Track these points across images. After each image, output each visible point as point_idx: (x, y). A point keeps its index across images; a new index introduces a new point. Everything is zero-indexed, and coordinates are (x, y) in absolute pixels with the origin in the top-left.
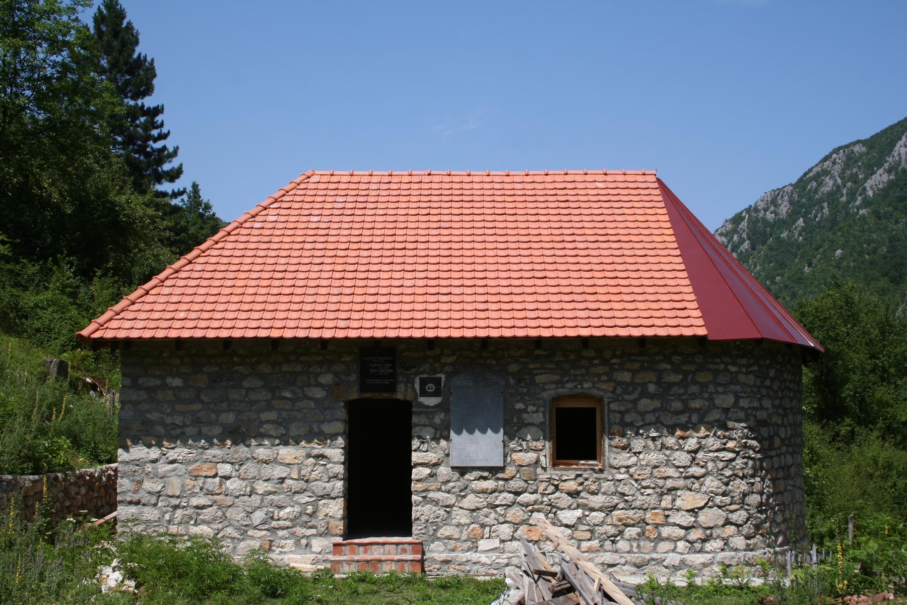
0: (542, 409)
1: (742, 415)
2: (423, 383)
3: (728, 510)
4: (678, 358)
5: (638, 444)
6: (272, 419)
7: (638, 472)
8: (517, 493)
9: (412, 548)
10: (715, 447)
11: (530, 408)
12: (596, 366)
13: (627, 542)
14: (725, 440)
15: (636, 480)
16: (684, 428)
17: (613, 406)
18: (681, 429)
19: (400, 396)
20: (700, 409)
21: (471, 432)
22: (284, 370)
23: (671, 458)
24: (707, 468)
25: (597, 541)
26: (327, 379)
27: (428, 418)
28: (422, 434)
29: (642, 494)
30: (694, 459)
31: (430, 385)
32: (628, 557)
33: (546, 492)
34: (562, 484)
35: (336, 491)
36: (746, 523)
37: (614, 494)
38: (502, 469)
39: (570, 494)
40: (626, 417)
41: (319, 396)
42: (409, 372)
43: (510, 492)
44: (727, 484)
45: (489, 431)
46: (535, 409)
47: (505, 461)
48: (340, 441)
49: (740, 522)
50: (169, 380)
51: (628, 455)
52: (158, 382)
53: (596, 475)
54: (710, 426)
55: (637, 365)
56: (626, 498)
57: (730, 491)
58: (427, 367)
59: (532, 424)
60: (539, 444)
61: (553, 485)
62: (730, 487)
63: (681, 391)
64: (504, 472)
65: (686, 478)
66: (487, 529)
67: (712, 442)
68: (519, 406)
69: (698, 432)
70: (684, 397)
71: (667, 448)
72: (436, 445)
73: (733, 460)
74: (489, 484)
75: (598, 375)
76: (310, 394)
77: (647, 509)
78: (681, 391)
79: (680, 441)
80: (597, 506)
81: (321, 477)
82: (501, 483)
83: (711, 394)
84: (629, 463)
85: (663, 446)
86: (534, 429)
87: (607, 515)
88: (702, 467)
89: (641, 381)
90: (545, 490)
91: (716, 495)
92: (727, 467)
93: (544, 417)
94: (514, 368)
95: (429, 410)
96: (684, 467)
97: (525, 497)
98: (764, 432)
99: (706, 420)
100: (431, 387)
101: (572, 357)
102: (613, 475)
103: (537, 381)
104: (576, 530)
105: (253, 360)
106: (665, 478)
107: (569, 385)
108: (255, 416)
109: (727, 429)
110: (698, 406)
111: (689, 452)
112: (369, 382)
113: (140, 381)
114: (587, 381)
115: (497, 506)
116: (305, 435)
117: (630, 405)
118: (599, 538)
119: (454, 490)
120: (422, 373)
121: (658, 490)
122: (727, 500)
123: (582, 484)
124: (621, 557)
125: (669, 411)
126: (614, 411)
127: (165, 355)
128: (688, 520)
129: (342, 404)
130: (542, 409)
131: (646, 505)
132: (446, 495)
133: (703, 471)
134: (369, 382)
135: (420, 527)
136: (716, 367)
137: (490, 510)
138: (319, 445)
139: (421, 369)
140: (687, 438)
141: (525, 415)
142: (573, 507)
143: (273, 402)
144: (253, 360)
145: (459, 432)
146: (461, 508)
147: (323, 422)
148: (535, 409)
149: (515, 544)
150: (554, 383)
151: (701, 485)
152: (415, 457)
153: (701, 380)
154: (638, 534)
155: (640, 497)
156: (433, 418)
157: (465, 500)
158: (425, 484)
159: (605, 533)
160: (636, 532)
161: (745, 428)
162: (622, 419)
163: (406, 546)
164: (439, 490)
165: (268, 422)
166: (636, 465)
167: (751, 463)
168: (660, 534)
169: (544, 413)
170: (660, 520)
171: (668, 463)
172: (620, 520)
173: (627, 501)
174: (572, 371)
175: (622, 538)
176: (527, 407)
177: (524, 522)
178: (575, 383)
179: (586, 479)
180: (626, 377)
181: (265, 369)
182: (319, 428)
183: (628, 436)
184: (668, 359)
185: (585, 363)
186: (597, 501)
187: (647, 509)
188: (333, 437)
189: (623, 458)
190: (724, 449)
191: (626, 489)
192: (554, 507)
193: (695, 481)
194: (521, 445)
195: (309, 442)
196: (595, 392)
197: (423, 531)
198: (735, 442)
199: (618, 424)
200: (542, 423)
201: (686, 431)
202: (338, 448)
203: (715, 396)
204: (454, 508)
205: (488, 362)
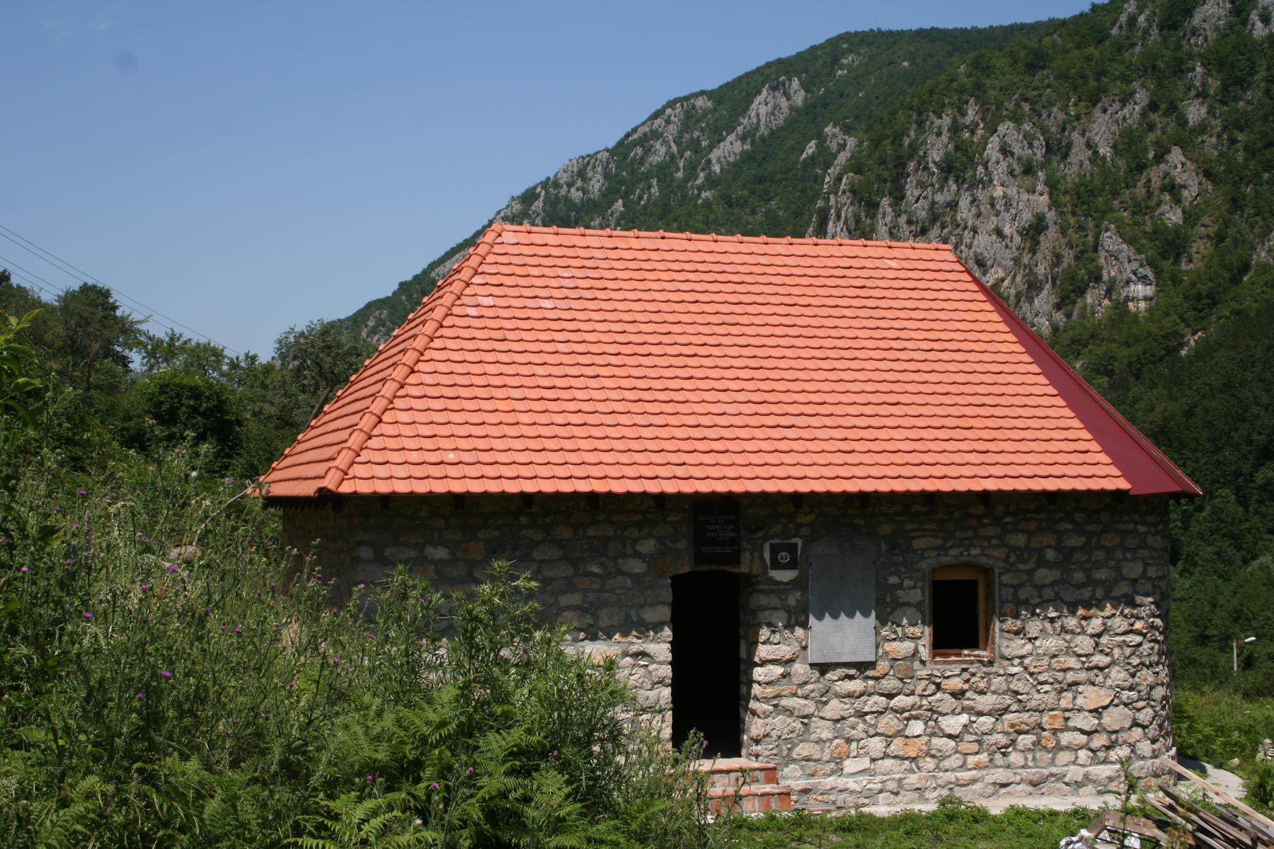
0: (920, 584)
2: (775, 550)
3: (1134, 708)
4: (1082, 515)
5: (1034, 627)
6: (575, 603)
7: (1034, 664)
8: (890, 696)
9: (766, 775)
10: (1122, 629)
11: (907, 583)
12: (985, 526)
13: (1021, 755)
14: (1132, 620)
15: (1031, 674)
16: (1088, 606)
17: (1006, 579)
18: (1084, 607)
19: (744, 569)
20: (1106, 581)
21: (835, 616)
22: (589, 534)
23: (1073, 645)
24: (1112, 656)
25: (985, 754)
26: (647, 546)
27: (780, 598)
28: (773, 620)
29: (1038, 691)
30: (1097, 644)
31: (783, 554)
32: (1024, 773)
33: (926, 693)
34: (945, 681)
35: (662, 702)
36: (1151, 723)
37: (1005, 693)
38: (872, 665)
40: (1020, 592)
41: (637, 570)
42: (756, 536)
43: (882, 695)
44: (1133, 676)
45: (858, 614)
46: (912, 583)
47: (877, 653)
48: (667, 632)
49: (1146, 723)
50: (429, 550)
51: (1023, 642)
53: (985, 669)
55: (1033, 525)
56: (1019, 697)
57: (1138, 684)
59: (909, 604)
60: (917, 630)
61: (934, 683)
62: (1136, 679)
63: (1084, 558)
64: (874, 669)
65: (1089, 669)
66: (854, 745)
67: (1119, 624)
68: (893, 580)
69: (1102, 610)
70: (1087, 566)
71: (1067, 632)
72: (790, 635)
73: (1140, 645)
74: (856, 685)
75: (988, 538)
76: (625, 569)
77: (1043, 711)
78: (1084, 558)
79: (1083, 622)
80: (986, 709)
81: (642, 683)
82: (871, 682)
83: (1118, 561)
84: (1023, 652)
85: (1064, 630)
86: (911, 611)
87: (997, 719)
88: (1107, 655)
89: (1038, 546)
90: (924, 690)
91: (1123, 689)
92: (1133, 654)
93: (923, 593)
94: (886, 529)
95: (782, 587)
96: (1086, 656)
97: (900, 701)
99: (1113, 595)
100: (784, 557)
101: (957, 515)
102: (1004, 669)
103: (915, 547)
104: (961, 741)
105: (548, 521)
107: (954, 552)
108: (552, 600)
109: (1134, 605)
110: (1103, 577)
111: (1092, 636)
112: (705, 550)
113: (388, 552)
114: (975, 547)
115: (867, 714)
116: (619, 626)
117: (1025, 577)
118: (988, 750)
119: (812, 695)
120: (773, 537)
121: (1057, 686)
122: (1133, 694)
123: (967, 681)
124: (1015, 774)
125: (1069, 583)
126: (1006, 585)
127: (423, 514)
128: (1088, 722)
129: (669, 581)
130: (920, 584)
131: (1043, 706)
132: (803, 702)
133: (1108, 660)
134: (705, 550)
135: (770, 746)
136: (1124, 527)
137: (857, 720)
138: (638, 638)
139: (771, 532)
140: (1090, 618)
141: (900, 593)
142: (957, 711)
143: (576, 580)
144: (548, 521)
145: (820, 617)
146: (822, 718)
147: (642, 607)
148: (912, 583)
149: (888, 763)
150: (936, 549)
151: (1105, 678)
152: (763, 652)
153: (1107, 544)
154: (1034, 744)
155: (1037, 696)
156: (786, 598)
157: (827, 707)
158: (776, 688)
159: (995, 744)
160: (1031, 741)
161: (1152, 603)
162: (1015, 594)
163: (757, 773)
164: (795, 695)
165: (569, 608)
166: (1031, 654)
167: (1157, 647)
168: (1058, 742)
169: (922, 588)
170: (1058, 724)
171: (1069, 651)
172: (1012, 726)
173: (1020, 701)
174: (957, 533)
175: (1015, 749)
176: (903, 581)
177: (899, 733)
178: (961, 549)
179: (973, 675)
180: (1020, 540)
181: (564, 533)
182: (639, 616)
183: (1022, 617)
186: (986, 702)
187: (1043, 711)
188: (657, 627)
189: (1018, 646)
190: (1131, 632)
191: (1016, 685)
192: (934, 712)
193: (1099, 673)
194: (895, 632)
195: (625, 634)
196: (984, 560)
197: (774, 752)
198: (1143, 622)
199: (1010, 602)
200: (921, 603)
201: (1089, 610)
202: (665, 642)
203: (1122, 563)
204: (814, 719)
205: (855, 521)
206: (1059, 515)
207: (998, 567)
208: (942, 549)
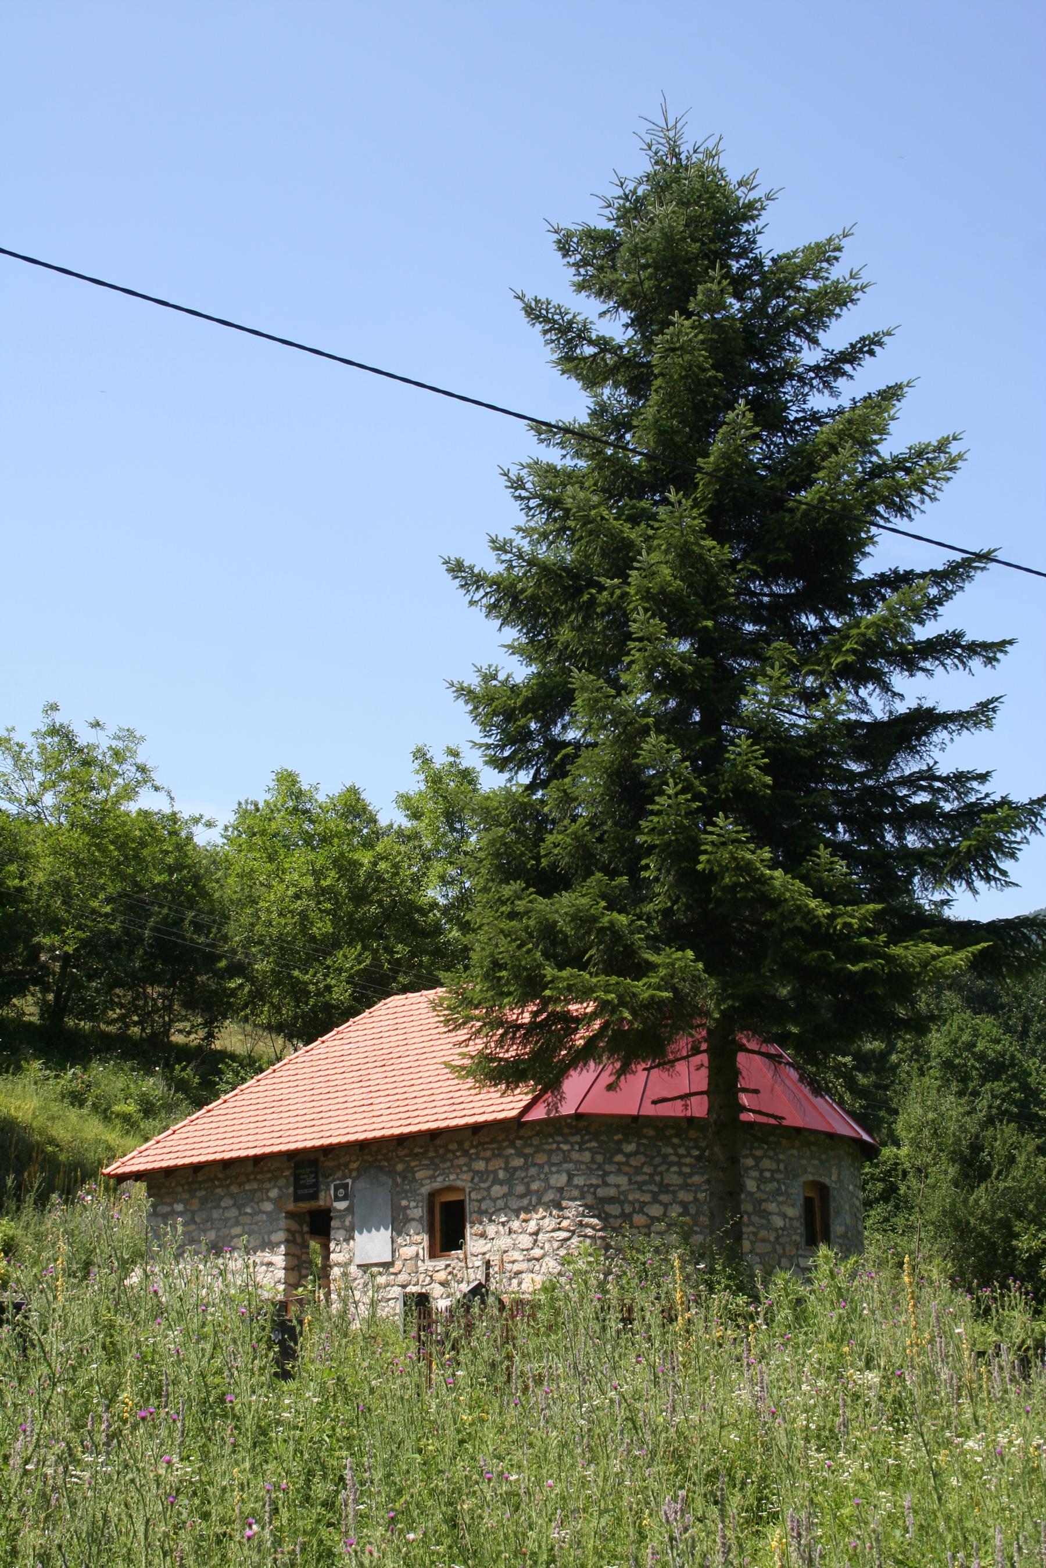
1: (576, 1193)
2: (336, 1190)
5: (491, 1230)
10: (549, 1228)
11: (413, 1204)
12: (457, 1157)
16: (527, 1211)
17: (474, 1196)
19: (321, 1203)
26: (274, 1193)
28: (337, 1236)
30: (536, 1241)
38: (390, 1264)
39: (442, 1284)
48: (283, 1248)
52: (169, 1209)
54: (547, 1206)
55: (489, 1153)
58: (339, 1174)
59: (413, 1219)
60: (418, 1238)
63: (523, 1174)
65: (529, 1260)
67: (549, 1223)
68: (404, 1203)
73: (568, 1239)
75: (460, 1167)
78: (523, 1174)
84: (485, 1250)
86: (414, 1224)
94: (400, 1167)
98: (614, 1209)
100: (341, 1192)
101: (441, 1151)
106: (513, 1262)
107: (440, 1179)
109: (561, 1208)
111: (531, 1234)
112: (300, 1192)
134: (300, 1192)
145: (361, 1233)
150: (430, 1178)
153: (539, 1161)
167: (588, 1241)
180: (480, 1165)
181: (234, 1189)
184: (512, 1145)
185: (450, 1156)
188: (278, 1244)
190: (559, 1229)
195: (263, 1251)
196: (459, 1183)
200: (421, 1217)
206: (505, 1144)
207: (468, 1186)
208: (433, 1178)
